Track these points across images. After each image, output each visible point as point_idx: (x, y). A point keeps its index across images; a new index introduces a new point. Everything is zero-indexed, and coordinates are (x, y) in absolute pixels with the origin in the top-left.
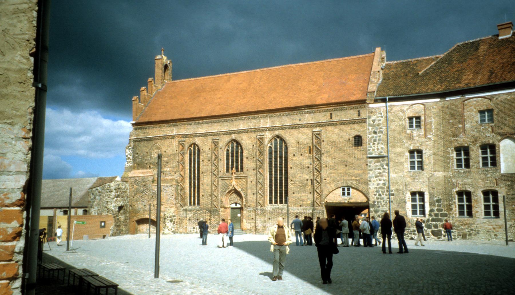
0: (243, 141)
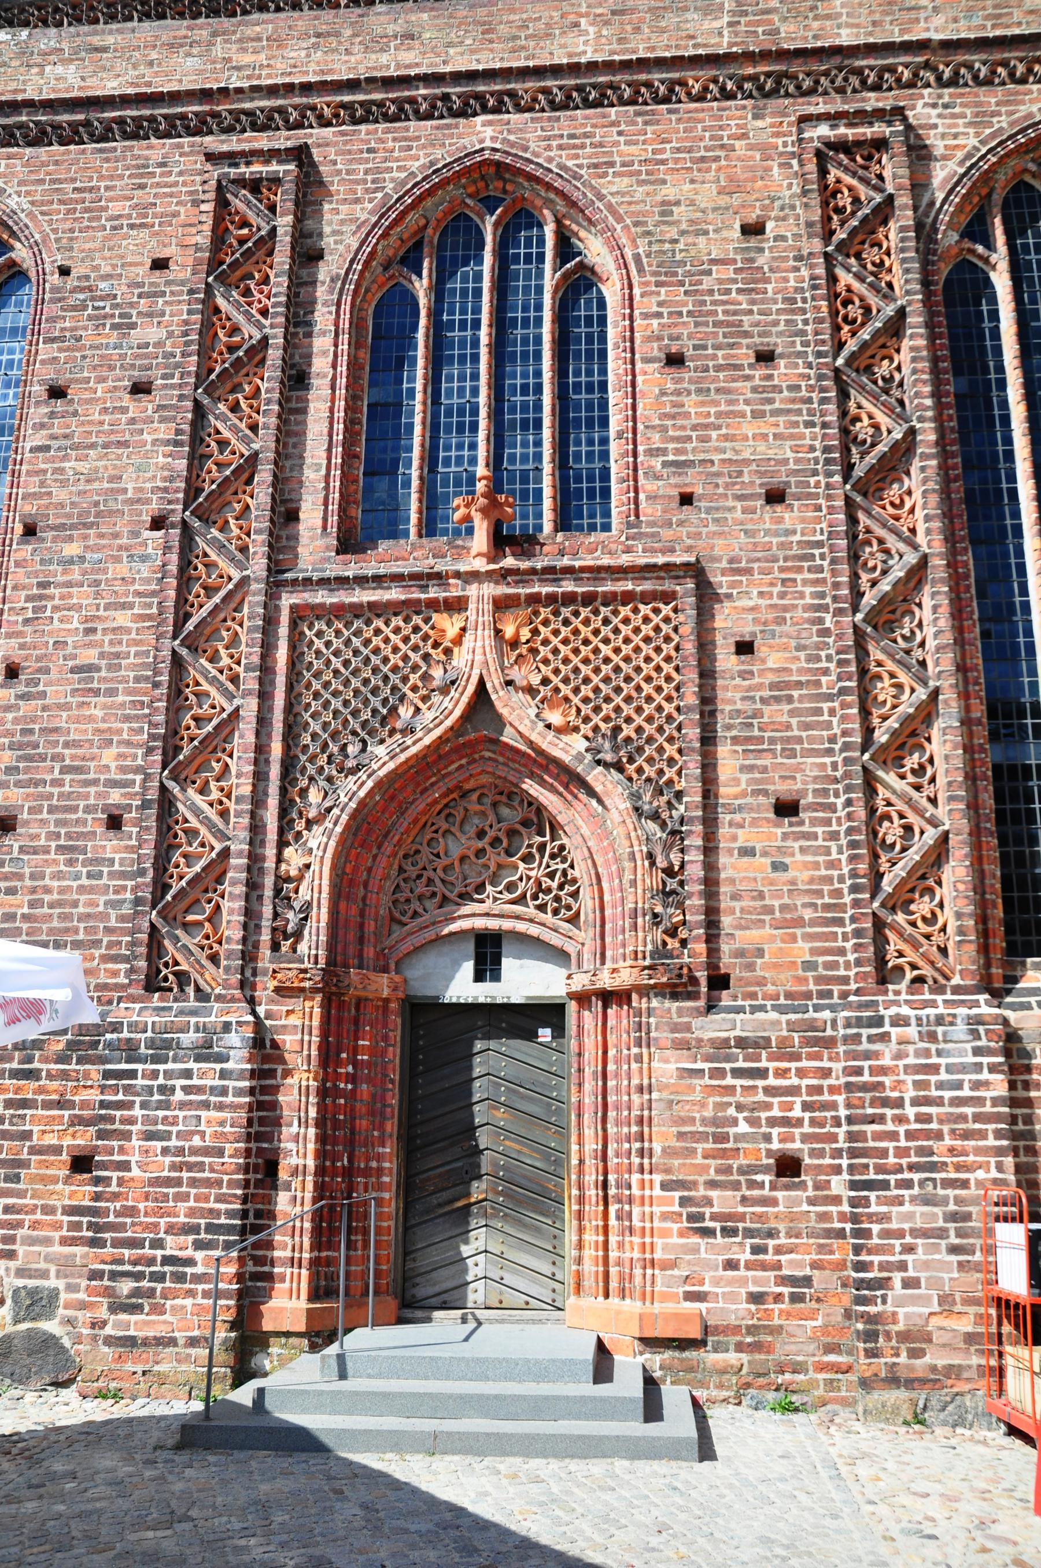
0: (613, 185)
